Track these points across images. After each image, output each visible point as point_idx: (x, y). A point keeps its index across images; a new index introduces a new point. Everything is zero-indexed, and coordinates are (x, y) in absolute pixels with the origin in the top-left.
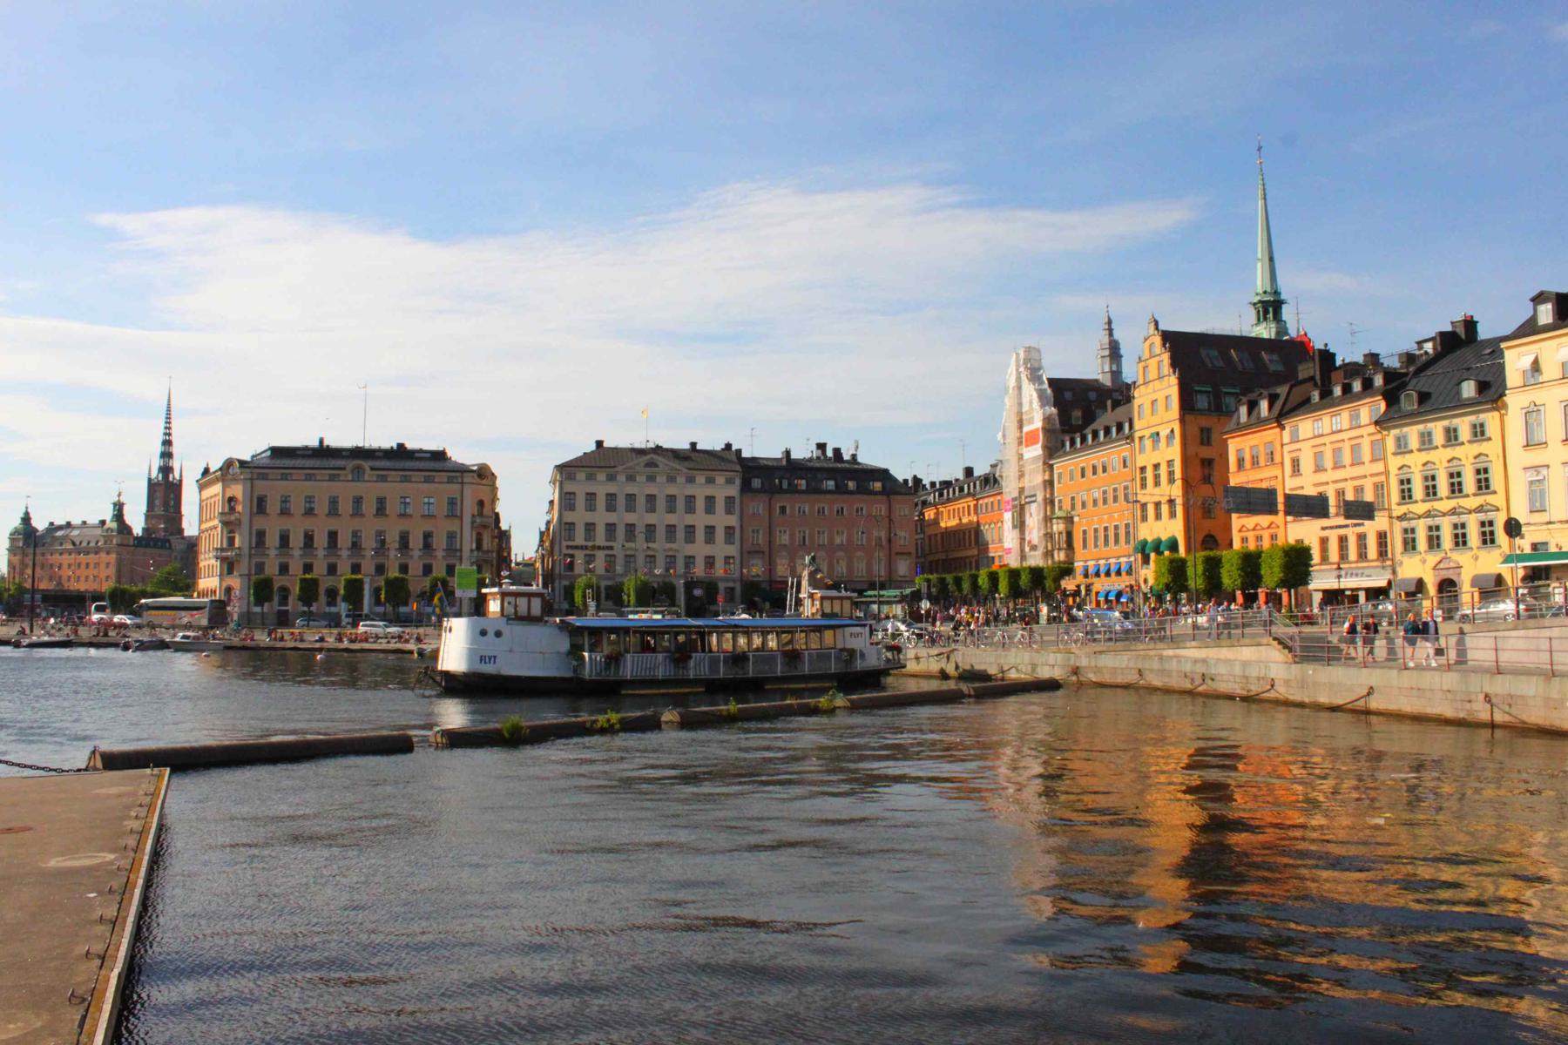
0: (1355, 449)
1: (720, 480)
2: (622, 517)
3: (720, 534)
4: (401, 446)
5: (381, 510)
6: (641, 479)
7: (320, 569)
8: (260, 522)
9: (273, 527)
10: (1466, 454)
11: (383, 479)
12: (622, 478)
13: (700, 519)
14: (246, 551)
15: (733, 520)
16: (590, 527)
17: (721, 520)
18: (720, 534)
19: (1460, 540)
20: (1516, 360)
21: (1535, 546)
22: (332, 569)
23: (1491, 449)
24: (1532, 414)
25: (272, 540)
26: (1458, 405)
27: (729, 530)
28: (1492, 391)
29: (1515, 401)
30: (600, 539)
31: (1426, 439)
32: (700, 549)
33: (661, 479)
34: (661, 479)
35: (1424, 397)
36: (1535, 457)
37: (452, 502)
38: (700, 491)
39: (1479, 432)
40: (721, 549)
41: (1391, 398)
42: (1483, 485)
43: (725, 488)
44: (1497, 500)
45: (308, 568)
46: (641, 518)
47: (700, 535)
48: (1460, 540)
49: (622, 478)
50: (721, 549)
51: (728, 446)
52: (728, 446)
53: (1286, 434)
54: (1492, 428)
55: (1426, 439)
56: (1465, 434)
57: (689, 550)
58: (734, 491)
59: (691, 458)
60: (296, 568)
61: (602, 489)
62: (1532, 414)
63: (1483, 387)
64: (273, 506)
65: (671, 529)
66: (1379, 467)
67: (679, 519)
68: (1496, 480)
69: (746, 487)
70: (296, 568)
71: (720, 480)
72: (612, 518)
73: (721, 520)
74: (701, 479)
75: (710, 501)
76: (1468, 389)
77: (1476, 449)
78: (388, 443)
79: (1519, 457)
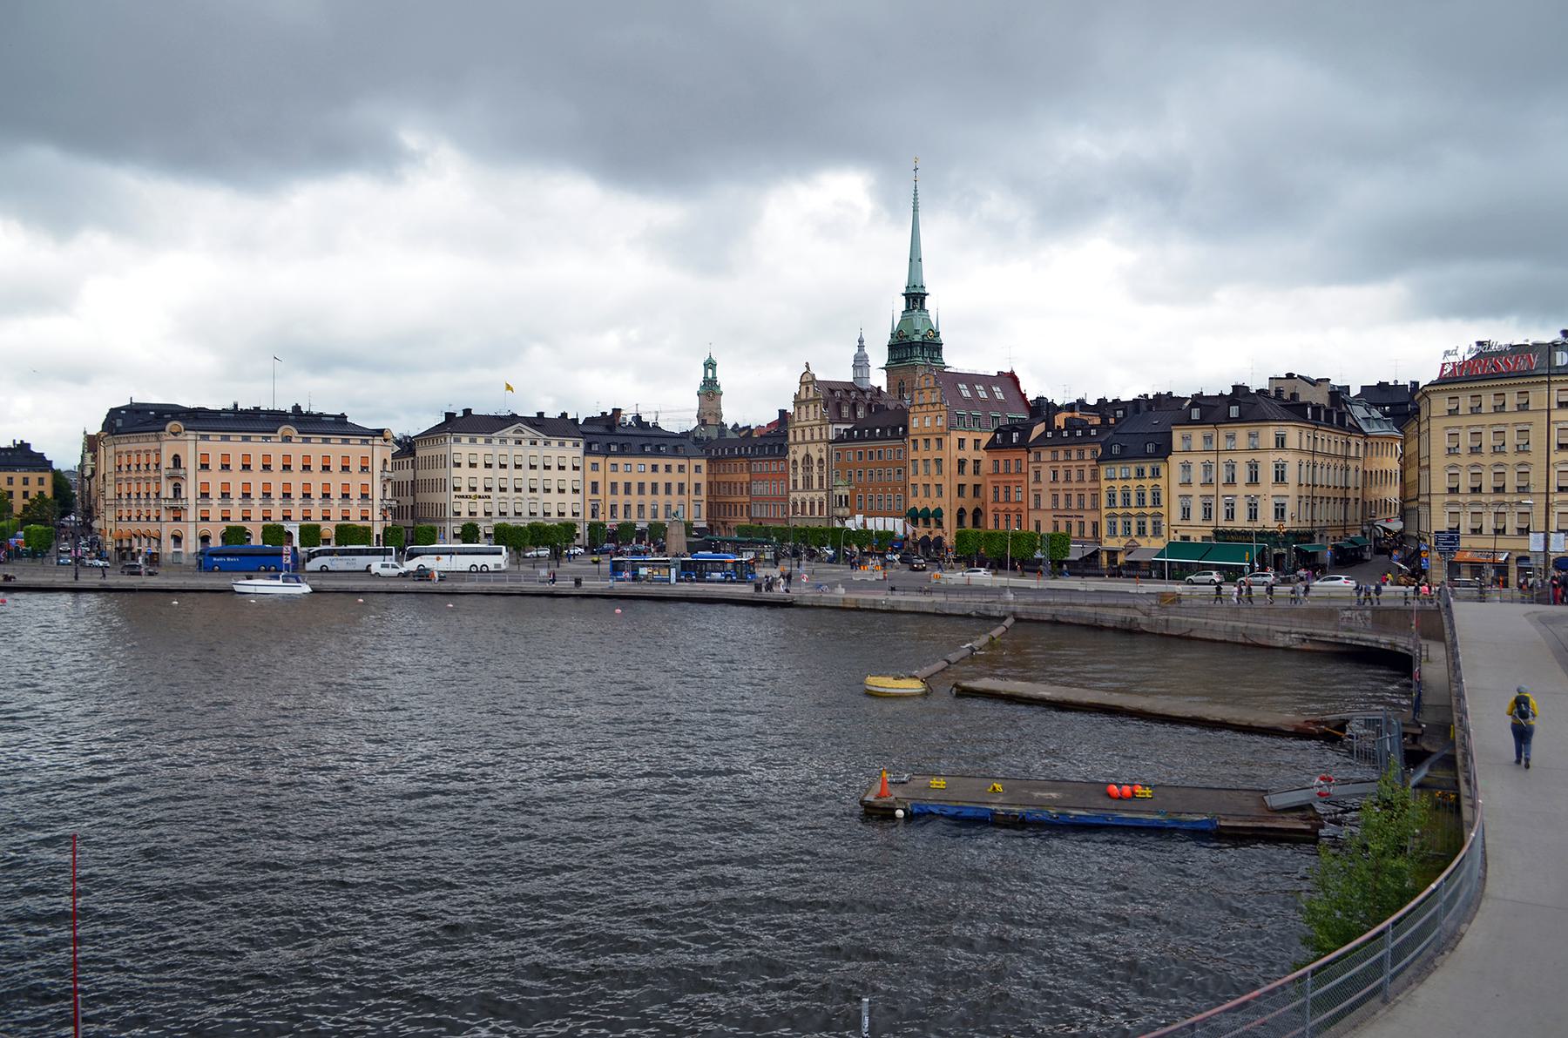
0: (1081, 472)
1: (569, 444)
4: (297, 408)
6: (511, 443)
10: (1148, 483)
11: (307, 440)
12: (496, 442)
14: (192, 501)
19: (1142, 532)
21: (1184, 538)
23: (1161, 482)
24: (1186, 467)
25: (215, 492)
28: (1164, 450)
33: (526, 443)
34: (526, 443)
36: (1185, 491)
37: (364, 459)
39: (1156, 473)
42: (1157, 502)
44: (1163, 511)
48: (1142, 532)
49: (496, 442)
51: (564, 415)
52: (564, 415)
53: (1032, 457)
54: (1163, 472)
56: (1148, 473)
58: (579, 452)
62: (1186, 467)
66: (1095, 485)
68: (1164, 501)
69: (588, 451)
71: (569, 444)
74: (555, 443)
77: (1153, 482)
79: (1176, 490)
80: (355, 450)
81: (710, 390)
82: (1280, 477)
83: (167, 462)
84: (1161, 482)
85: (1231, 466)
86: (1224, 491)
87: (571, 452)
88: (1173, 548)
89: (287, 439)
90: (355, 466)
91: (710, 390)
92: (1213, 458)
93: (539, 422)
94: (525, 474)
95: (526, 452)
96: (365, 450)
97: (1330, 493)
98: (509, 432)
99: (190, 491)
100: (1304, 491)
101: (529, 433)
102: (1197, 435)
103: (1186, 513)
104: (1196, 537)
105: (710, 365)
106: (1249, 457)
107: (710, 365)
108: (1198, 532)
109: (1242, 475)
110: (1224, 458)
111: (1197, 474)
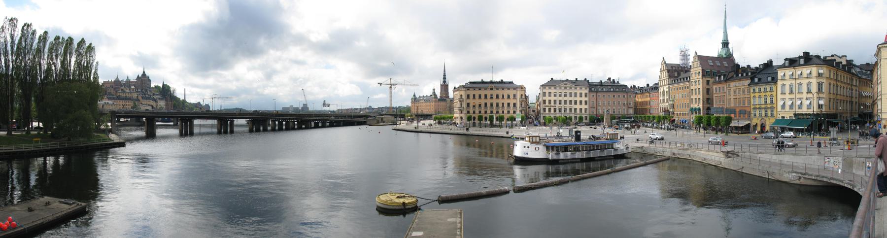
2: (558, 98)
3: (583, 103)
7: (483, 112)
8: (468, 101)
9: (471, 101)
13: (578, 99)
15: (587, 99)
16: (550, 101)
17: (584, 99)
18: (583, 103)
20: (780, 73)
22: (486, 112)
23: (774, 93)
24: (783, 86)
27: (586, 102)
28: (774, 80)
29: (780, 83)
30: (552, 104)
31: (760, 90)
32: (578, 106)
35: (759, 80)
36: (783, 97)
38: (578, 91)
39: (771, 90)
40: (584, 107)
41: (752, 79)
42: (772, 102)
43: (585, 91)
45: (480, 112)
46: (563, 98)
47: (578, 103)
50: (584, 107)
54: (774, 89)
55: (760, 90)
57: (576, 106)
58: (587, 91)
59: (576, 83)
60: (477, 112)
61: (553, 91)
62: (783, 86)
63: (773, 78)
64: (471, 97)
65: (571, 101)
67: (573, 99)
69: (590, 91)
70: (477, 112)
72: (555, 98)
73: (584, 99)
75: (581, 94)
76: (770, 79)
78: (498, 80)
79: (780, 96)
82: (820, 90)
84: (774, 93)
85: (800, 84)
86: (798, 96)
88: (778, 121)
89: (492, 89)
90: (512, 97)
92: (793, 82)
95: (568, 91)
96: (515, 92)
97: (844, 98)
98: (562, 85)
100: (832, 96)
101: (569, 85)
103: (783, 106)
104: (787, 116)
106: (808, 81)
108: (788, 115)
109: (805, 89)
110: (798, 81)
111: (787, 90)
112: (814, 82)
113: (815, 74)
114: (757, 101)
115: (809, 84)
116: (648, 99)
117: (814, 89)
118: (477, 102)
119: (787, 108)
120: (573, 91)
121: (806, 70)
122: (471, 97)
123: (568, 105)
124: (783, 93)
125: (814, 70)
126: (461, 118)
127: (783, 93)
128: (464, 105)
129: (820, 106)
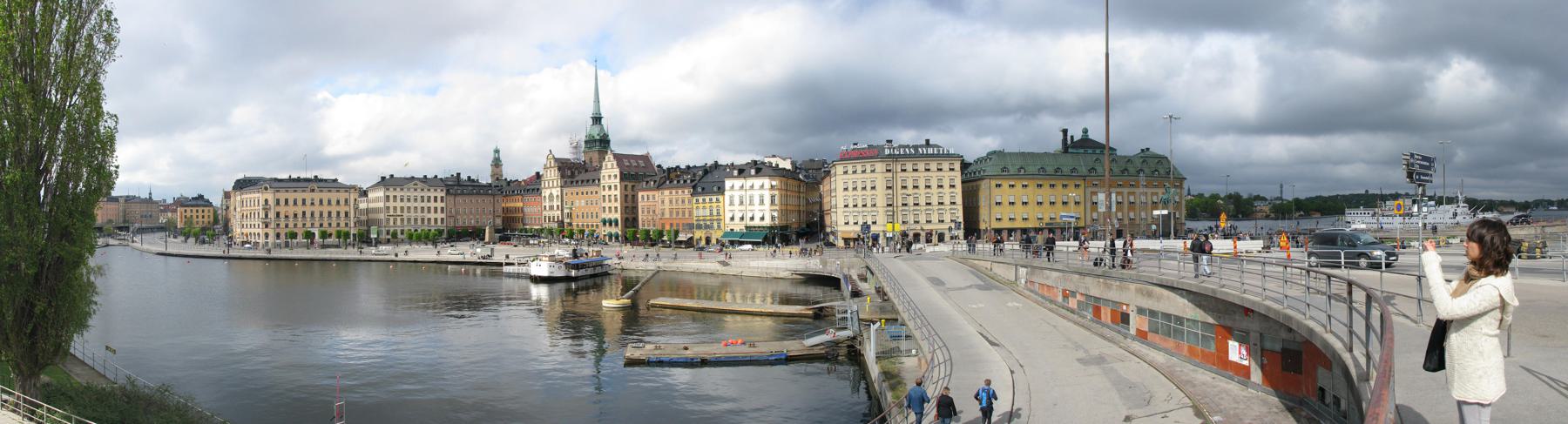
2: (406, 204)
5: (329, 202)
13: (432, 204)
17: (439, 205)
20: (728, 183)
26: (713, 193)
28: (721, 190)
29: (727, 194)
32: (432, 216)
40: (440, 216)
46: (412, 204)
50: (440, 216)
61: (399, 194)
64: (282, 202)
67: (425, 205)
69: (448, 192)
73: (439, 205)
79: (727, 208)
80: (342, 196)
81: (497, 163)
82: (772, 202)
83: (262, 202)
87: (440, 194)
88: (726, 235)
91: (497, 163)
93: (425, 179)
94: (419, 204)
95: (419, 194)
98: (411, 185)
99: (272, 215)
101: (420, 185)
102: (738, 183)
104: (737, 229)
105: (497, 151)
107: (497, 151)
108: (739, 227)
109: (757, 200)
111: (737, 201)
112: (767, 195)
113: (767, 186)
114: (701, 212)
115: (762, 197)
116: (520, 205)
117: (767, 200)
118: (291, 210)
119: (737, 219)
120: (426, 194)
121: (758, 182)
122: (282, 202)
123: (419, 215)
124: (732, 204)
125: (767, 182)
126: (267, 235)
127: (732, 204)
128: (272, 215)
129: (773, 218)
